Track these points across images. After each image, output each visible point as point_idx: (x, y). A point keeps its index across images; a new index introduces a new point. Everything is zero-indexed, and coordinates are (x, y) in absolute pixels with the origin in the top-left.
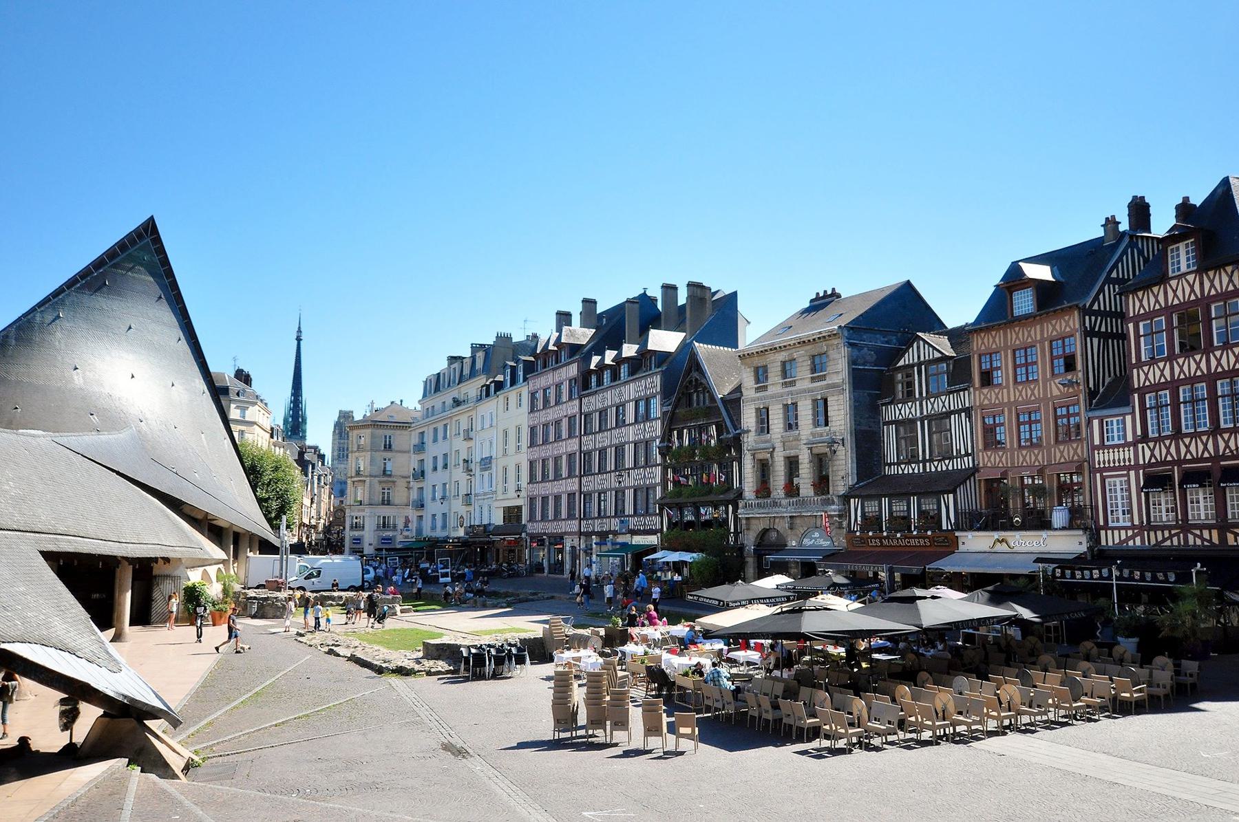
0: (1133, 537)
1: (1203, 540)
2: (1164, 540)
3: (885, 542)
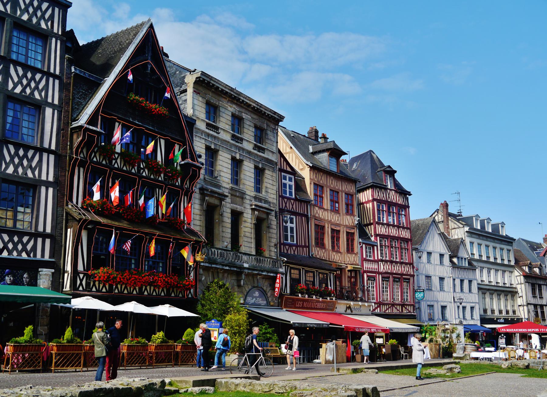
1: (397, 310)
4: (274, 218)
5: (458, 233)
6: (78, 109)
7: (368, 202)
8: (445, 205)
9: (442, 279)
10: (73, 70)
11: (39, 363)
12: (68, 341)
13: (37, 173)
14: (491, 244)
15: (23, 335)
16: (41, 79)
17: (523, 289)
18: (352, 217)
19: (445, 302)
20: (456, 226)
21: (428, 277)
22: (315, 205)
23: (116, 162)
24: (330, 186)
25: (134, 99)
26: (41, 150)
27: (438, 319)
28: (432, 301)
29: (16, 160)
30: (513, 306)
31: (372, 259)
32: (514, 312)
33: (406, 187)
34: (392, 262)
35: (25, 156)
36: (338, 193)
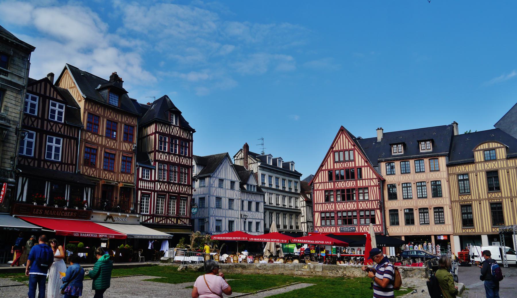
0: (150, 219)
1: (172, 222)
2: (160, 221)
3: (47, 212)
4: (13, 134)
5: (254, 167)
7: (151, 134)
8: (246, 146)
9: (231, 200)
14: (281, 177)
17: (304, 211)
18: (131, 145)
19: (233, 217)
20: (252, 162)
21: (219, 199)
22: (87, 131)
24: (107, 117)
27: (225, 230)
28: (221, 217)
30: (297, 223)
31: (149, 179)
32: (297, 227)
33: (192, 125)
34: (169, 183)
36: (117, 123)
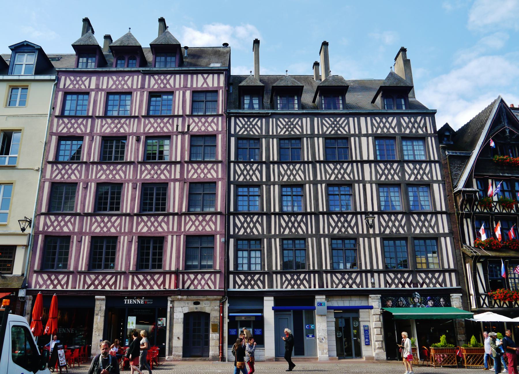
6: (456, 179)
10: (447, 153)
11: (455, 361)
12: (474, 346)
13: (436, 229)
15: (439, 341)
16: (426, 167)
23: (496, 208)
25: (499, 159)
26: (435, 213)
29: (420, 224)
35: (426, 219)
